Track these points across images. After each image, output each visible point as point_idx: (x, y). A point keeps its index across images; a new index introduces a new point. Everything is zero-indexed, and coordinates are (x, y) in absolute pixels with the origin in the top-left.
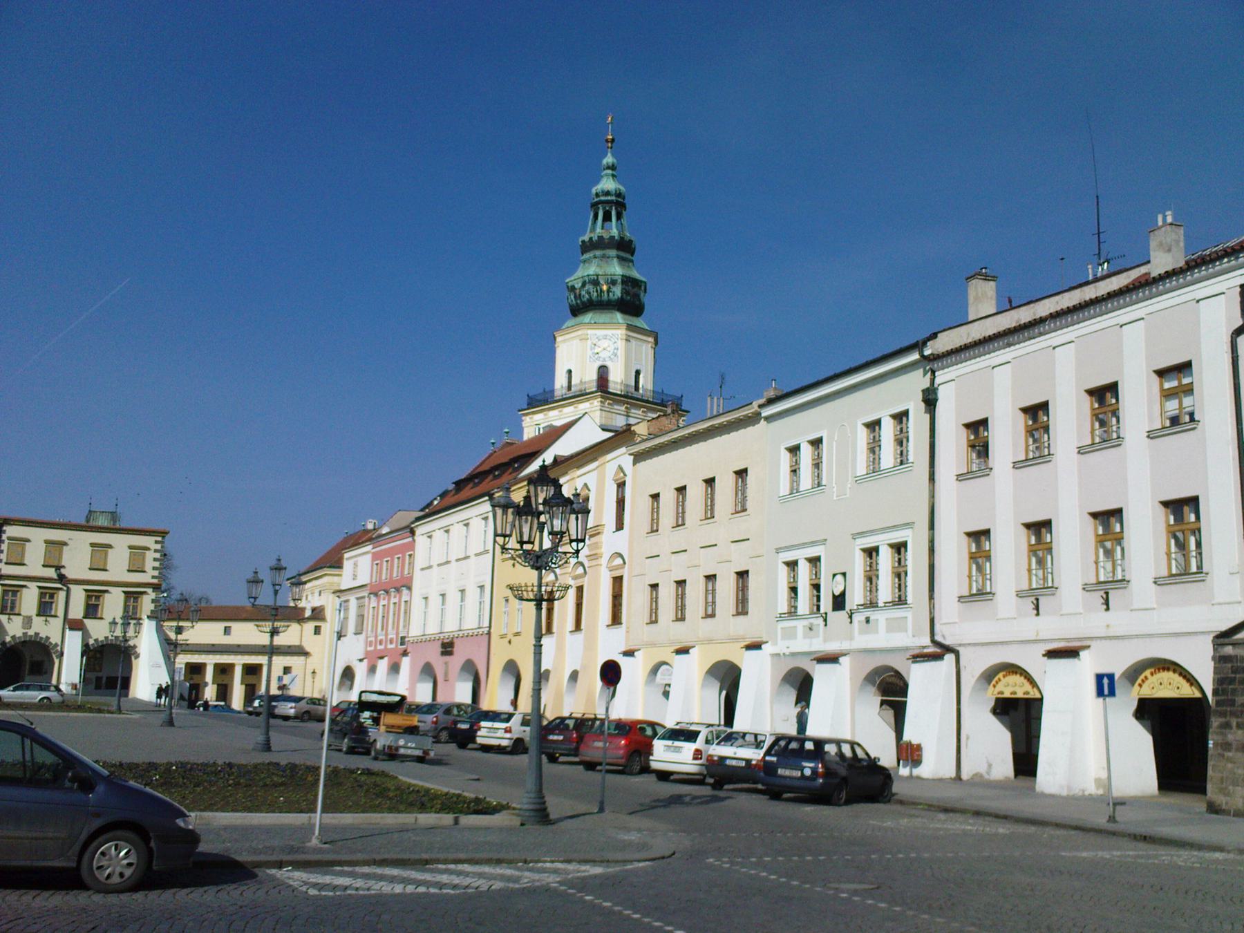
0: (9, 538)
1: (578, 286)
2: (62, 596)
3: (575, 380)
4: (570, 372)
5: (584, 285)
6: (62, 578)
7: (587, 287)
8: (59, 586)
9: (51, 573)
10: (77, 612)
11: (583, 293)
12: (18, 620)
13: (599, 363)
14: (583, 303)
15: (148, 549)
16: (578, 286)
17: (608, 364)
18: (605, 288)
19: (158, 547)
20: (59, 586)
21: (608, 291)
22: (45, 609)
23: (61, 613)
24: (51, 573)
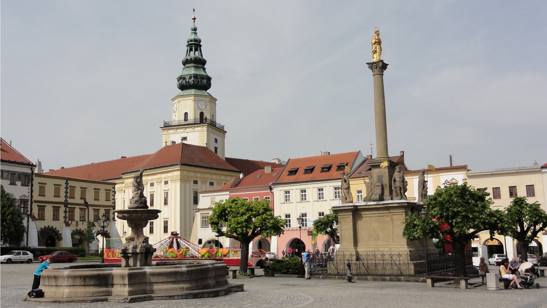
0: (70, 186)
1: (187, 78)
2: (87, 211)
3: (191, 117)
4: (186, 114)
5: (190, 78)
6: (86, 204)
7: (193, 79)
8: (85, 207)
9: (82, 202)
10: (92, 219)
11: (190, 81)
12: (74, 223)
13: (200, 111)
14: (189, 85)
15: (110, 190)
16: (187, 78)
17: (204, 111)
18: (200, 80)
19: (113, 190)
20: (85, 207)
21: (201, 82)
22: (83, 219)
23: (87, 219)
24: (82, 202)
